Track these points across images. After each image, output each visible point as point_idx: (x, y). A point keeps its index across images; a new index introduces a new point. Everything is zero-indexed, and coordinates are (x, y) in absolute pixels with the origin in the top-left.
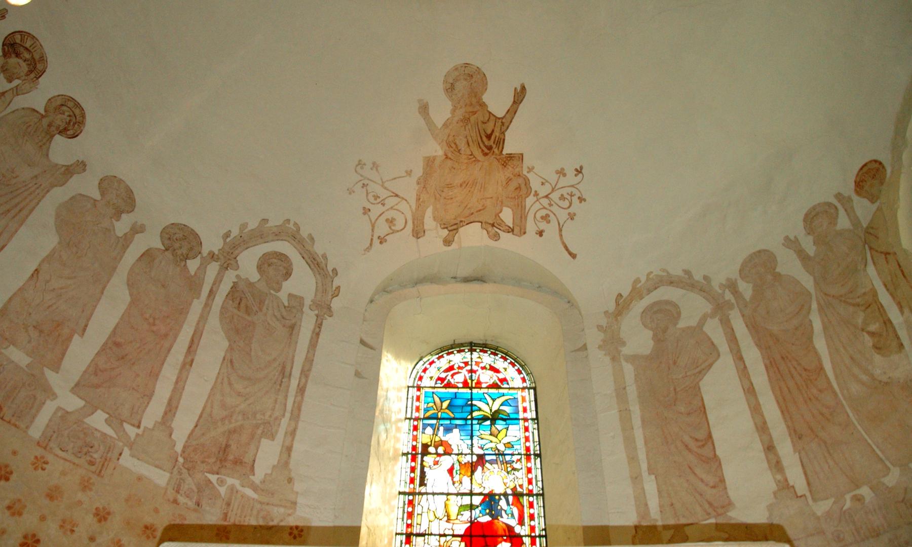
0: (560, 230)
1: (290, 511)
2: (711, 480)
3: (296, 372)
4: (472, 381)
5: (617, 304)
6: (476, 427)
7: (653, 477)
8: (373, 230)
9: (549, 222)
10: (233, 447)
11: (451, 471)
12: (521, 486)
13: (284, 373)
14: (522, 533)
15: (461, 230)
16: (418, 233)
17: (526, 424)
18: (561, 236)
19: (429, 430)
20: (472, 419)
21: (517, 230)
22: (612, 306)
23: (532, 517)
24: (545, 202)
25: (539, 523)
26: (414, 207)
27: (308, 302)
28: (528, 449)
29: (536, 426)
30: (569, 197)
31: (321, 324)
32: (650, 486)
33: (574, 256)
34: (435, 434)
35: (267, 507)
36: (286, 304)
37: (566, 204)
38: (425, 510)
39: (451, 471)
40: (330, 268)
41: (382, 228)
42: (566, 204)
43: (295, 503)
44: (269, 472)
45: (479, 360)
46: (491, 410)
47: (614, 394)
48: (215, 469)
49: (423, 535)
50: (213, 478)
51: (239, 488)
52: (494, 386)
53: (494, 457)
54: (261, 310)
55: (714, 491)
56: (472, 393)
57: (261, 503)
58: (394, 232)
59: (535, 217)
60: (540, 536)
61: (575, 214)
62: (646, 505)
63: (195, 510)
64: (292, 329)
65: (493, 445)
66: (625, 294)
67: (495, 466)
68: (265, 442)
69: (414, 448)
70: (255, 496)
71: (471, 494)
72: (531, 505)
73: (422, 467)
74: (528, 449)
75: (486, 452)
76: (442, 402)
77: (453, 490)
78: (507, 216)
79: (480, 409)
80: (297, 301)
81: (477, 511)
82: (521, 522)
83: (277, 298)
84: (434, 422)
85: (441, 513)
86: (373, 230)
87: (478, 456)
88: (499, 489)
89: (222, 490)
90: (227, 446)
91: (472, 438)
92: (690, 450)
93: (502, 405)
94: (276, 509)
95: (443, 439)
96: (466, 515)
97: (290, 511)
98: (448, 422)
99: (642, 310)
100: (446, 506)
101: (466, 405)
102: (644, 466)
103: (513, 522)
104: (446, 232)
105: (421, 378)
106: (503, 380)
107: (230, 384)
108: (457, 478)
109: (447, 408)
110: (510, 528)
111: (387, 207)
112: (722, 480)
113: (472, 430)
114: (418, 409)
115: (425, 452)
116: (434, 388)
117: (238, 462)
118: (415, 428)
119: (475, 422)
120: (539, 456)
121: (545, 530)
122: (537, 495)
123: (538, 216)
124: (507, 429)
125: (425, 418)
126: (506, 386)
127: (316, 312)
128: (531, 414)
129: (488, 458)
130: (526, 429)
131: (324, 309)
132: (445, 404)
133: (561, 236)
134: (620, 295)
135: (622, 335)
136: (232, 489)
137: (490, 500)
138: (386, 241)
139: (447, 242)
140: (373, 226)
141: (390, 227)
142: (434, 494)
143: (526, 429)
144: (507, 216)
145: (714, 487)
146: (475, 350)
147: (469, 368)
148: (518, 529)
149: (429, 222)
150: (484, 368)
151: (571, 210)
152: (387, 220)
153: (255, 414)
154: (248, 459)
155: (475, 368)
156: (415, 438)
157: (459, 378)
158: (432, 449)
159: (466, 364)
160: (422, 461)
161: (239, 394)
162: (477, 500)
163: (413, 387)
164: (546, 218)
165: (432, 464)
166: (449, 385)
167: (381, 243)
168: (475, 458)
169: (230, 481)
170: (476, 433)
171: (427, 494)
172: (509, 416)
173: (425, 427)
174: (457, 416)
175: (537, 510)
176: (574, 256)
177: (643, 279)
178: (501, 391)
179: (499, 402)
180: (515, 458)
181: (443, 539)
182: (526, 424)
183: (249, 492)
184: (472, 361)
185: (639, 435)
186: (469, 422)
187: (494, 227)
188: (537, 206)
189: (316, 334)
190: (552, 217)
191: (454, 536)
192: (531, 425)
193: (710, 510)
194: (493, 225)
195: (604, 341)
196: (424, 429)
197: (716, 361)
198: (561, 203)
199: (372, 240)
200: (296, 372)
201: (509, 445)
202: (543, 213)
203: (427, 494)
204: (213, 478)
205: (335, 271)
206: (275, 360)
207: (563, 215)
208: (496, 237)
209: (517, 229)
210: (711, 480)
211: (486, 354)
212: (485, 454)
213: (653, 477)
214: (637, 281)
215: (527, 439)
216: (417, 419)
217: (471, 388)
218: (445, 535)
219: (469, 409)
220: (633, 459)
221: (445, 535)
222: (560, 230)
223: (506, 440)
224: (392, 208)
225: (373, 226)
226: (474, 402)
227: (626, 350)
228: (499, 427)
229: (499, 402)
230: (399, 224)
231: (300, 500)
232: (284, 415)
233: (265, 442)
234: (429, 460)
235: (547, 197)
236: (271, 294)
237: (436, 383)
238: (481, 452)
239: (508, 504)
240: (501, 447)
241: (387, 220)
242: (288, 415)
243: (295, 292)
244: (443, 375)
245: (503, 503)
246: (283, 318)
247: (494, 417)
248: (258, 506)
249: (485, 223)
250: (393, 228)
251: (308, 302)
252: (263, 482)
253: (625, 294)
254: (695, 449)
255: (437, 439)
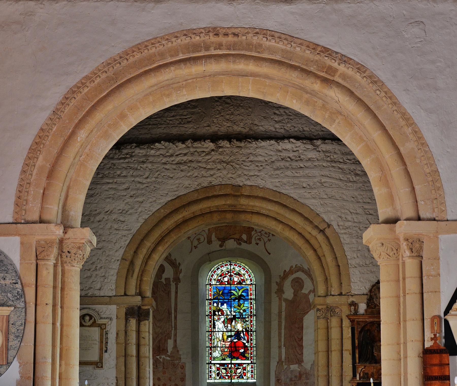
0: (265, 244)
1: (179, 361)
2: (300, 353)
3: (173, 312)
4: (231, 281)
5: (284, 274)
6: (233, 302)
7: (285, 348)
8: (192, 244)
9: (260, 241)
10: (161, 345)
11: (223, 322)
12: (248, 328)
13: (170, 313)
14: (248, 346)
15: (226, 242)
16: (210, 242)
17: (251, 301)
18: (265, 246)
19: (215, 305)
20: (231, 299)
21: (248, 242)
22: (282, 275)
23: (251, 340)
24: (259, 234)
25: (254, 342)
26: (207, 233)
27: (171, 280)
28: (251, 312)
29: (255, 302)
30: (268, 234)
31: (177, 287)
32: (283, 350)
33: (269, 254)
34: (218, 306)
35: (173, 361)
36: (165, 283)
37: (267, 236)
38: (216, 338)
39: (223, 322)
40: (177, 263)
41: (195, 243)
42: (267, 236)
43: (180, 358)
44: (172, 350)
45: (233, 270)
46: (238, 295)
47: (278, 314)
48: (158, 354)
49: (214, 347)
50: (158, 357)
51: (166, 358)
52: (240, 283)
53: (239, 316)
54: (158, 290)
55: (300, 356)
56: (231, 287)
57: (172, 360)
58: (200, 243)
59: (255, 238)
60: (254, 347)
61: (270, 240)
62: (281, 356)
63: (156, 368)
64: (169, 293)
65: (238, 311)
66: (287, 271)
67: (239, 319)
68: (169, 341)
69: (210, 312)
70: (170, 359)
71: (231, 331)
72: (251, 335)
73: (214, 320)
74: (251, 312)
75: (237, 314)
76: (220, 292)
77: (225, 330)
78: (244, 237)
79: (234, 295)
80: (167, 280)
81: (233, 338)
82: (248, 342)
83: (162, 282)
84: (217, 301)
85: (221, 338)
86: (192, 244)
87: (233, 315)
88: (241, 329)
89: (161, 360)
90: (160, 346)
91: (231, 308)
92: (296, 341)
93: (242, 292)
94: (176, 361)
95: (221, 308)
96: (230, 339)
97: (179, 361)
98: (222, 300)
99: (292, 279)
100: (223, 336)
101: (229, 293)
102: (283, 344)
103: (245, 342)
104: (220, 242)
105: (211, 280)
106: (243, 281)
107: (156, 325)
108: (226, 325)
109: (222, 294)
110: (244, 344)
111: (197, 234)
112: (302, 353)
113: (231, 304)
114: (211, 296)
115: (215, 315)
116: (216, 285)
117: (163, 350)
118: (210, 304)
119: (232, 300)
120: (255, 315)
121: (256, 344)
122: (254, 331)
123: (256, 238)
124: (244, 303)
125: (214, 299)
126: (244, 283)
127: (175, 283)
128: (253, 297)
129: (237, 316)
130: (251, 303)
131: (177, 280)
132: (221, 293)
133: (265, 246)
134: (285, 271)
135: (284, 289)
136: (164, 359)
137: (238, 334)
138: (197, 247)
139: (221, 246)
140: (192, 242)
141: (198, 242)
142: (218, 331)
143: (251, 303)
144: (244, 237)
145: (300, 355)
146: (232, 265)
147: (229, 274)
148: (247, 344)
149: (213, 238)
150: (235, 274)
151: (269, 238)
152: (197, 239)
153: (164, 332)
154: (165, 348)
155: (232, 274)
156: (210, 308)
157: (226, 279)
158: (217, 313)
159: (228, 272)
160: (214, 318)
161: (159, 327)
162: (233, 333)
163: (208, 285)
164: (259, 239)
165: (217, 319)
166: (222, 283)
167: (195, 248)
168: (232, 316)
169: (163, 356)
170: (233, 305)
171: (216, 331)
172: (245, 297)
173: (214, 303)
174: (226, 298)
175: (254, 337)
176: (269, 254)
177: (294, 267)
178: (242, 286)
179: (241, 291)
180: (246, 316)
181: (222, 348)
182: (251, 301)
183: (168, 358)
184: (231, 271)
185: (283, 331)
186: (230, 300)
187: (239, 241)
188: (256, 235)
189: (176, 293)
190: (262, 239)
191: (225, 347)
192: (254, 302)
193: (298, 362)
194: (239, 240)
195: (278, 290)
196: (213, 304)
197: (310, 311)
198: (265, 235)
199: (192, 248)
200: (173, 312)
201: (244, 311)
202: (259, 237)
203: (216, 331)
204: (158, 357)
205: (179, 264)
206: (166, 309)
207: (266, 239)
208: (240, 244)
209: (249, 241)
210: (300, 353)
211: (237, 267)
212: (236, 315)
213: (285, 348)
214: (292, 267)
215: (251, 307)
216: (211, 300)
217: (231, 285)
218: (223, 347)
219: (230, 294)
220: (280, 340)
221: (223, 347)
222: (265, 244)
223: (243, 309)
224: (199, 234)
225: (192, 242)
226: (232, 291)
227: (285, 296)
228: (241, 302)
229: (241, 291)
230: (202, 239)
231: (182, 357)
232: (172, 329)
233: (169, 341)
234: (216, 318)
235: (260, 232)
236: (159, 281)
237: (217, 283)
238: (234, 314)
239: (243, 335)
240: (242, 311)
241: (197, 239)
242: (173, 329)
243: (167, 277)
244: (220, 278)
245: (242, 335)
246: (165, 290)
247: (240, 298)
248: (171, 362)
249: (236, 239)
250: (200, 242)
251: (171, 280)
252: (171, 354)
253: (287, 271)
254: (297, 340)
255: (218, 308)
